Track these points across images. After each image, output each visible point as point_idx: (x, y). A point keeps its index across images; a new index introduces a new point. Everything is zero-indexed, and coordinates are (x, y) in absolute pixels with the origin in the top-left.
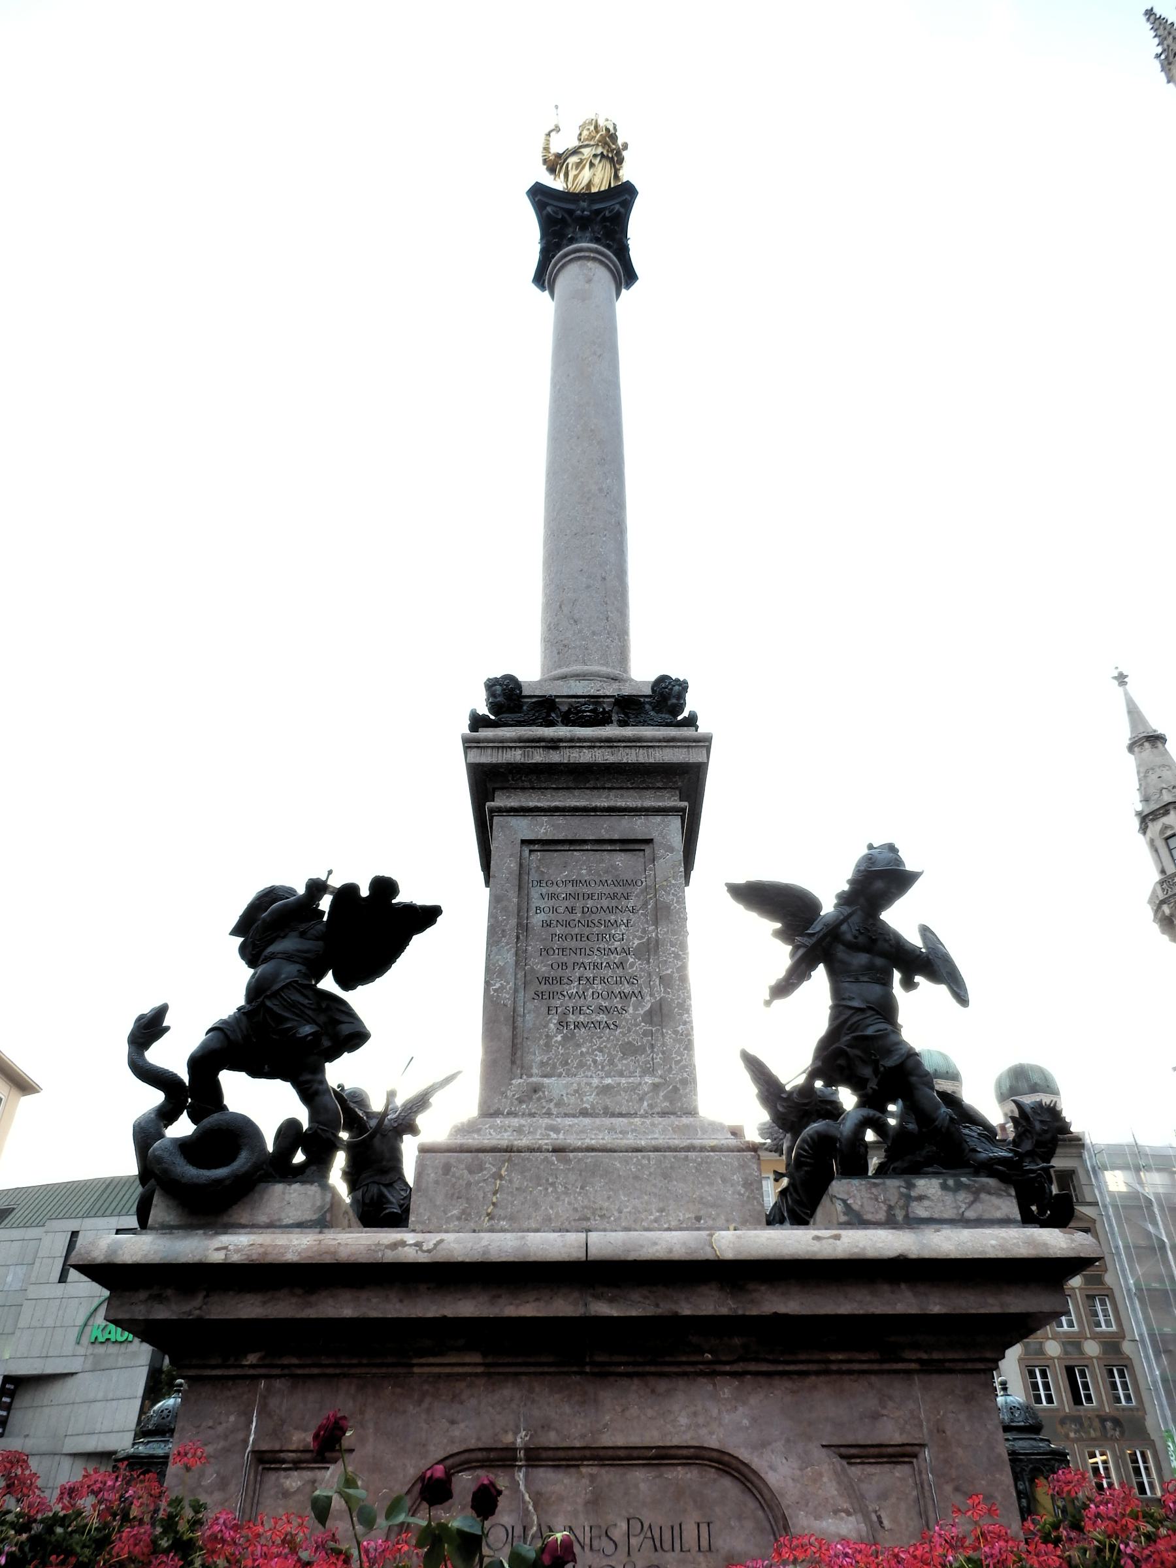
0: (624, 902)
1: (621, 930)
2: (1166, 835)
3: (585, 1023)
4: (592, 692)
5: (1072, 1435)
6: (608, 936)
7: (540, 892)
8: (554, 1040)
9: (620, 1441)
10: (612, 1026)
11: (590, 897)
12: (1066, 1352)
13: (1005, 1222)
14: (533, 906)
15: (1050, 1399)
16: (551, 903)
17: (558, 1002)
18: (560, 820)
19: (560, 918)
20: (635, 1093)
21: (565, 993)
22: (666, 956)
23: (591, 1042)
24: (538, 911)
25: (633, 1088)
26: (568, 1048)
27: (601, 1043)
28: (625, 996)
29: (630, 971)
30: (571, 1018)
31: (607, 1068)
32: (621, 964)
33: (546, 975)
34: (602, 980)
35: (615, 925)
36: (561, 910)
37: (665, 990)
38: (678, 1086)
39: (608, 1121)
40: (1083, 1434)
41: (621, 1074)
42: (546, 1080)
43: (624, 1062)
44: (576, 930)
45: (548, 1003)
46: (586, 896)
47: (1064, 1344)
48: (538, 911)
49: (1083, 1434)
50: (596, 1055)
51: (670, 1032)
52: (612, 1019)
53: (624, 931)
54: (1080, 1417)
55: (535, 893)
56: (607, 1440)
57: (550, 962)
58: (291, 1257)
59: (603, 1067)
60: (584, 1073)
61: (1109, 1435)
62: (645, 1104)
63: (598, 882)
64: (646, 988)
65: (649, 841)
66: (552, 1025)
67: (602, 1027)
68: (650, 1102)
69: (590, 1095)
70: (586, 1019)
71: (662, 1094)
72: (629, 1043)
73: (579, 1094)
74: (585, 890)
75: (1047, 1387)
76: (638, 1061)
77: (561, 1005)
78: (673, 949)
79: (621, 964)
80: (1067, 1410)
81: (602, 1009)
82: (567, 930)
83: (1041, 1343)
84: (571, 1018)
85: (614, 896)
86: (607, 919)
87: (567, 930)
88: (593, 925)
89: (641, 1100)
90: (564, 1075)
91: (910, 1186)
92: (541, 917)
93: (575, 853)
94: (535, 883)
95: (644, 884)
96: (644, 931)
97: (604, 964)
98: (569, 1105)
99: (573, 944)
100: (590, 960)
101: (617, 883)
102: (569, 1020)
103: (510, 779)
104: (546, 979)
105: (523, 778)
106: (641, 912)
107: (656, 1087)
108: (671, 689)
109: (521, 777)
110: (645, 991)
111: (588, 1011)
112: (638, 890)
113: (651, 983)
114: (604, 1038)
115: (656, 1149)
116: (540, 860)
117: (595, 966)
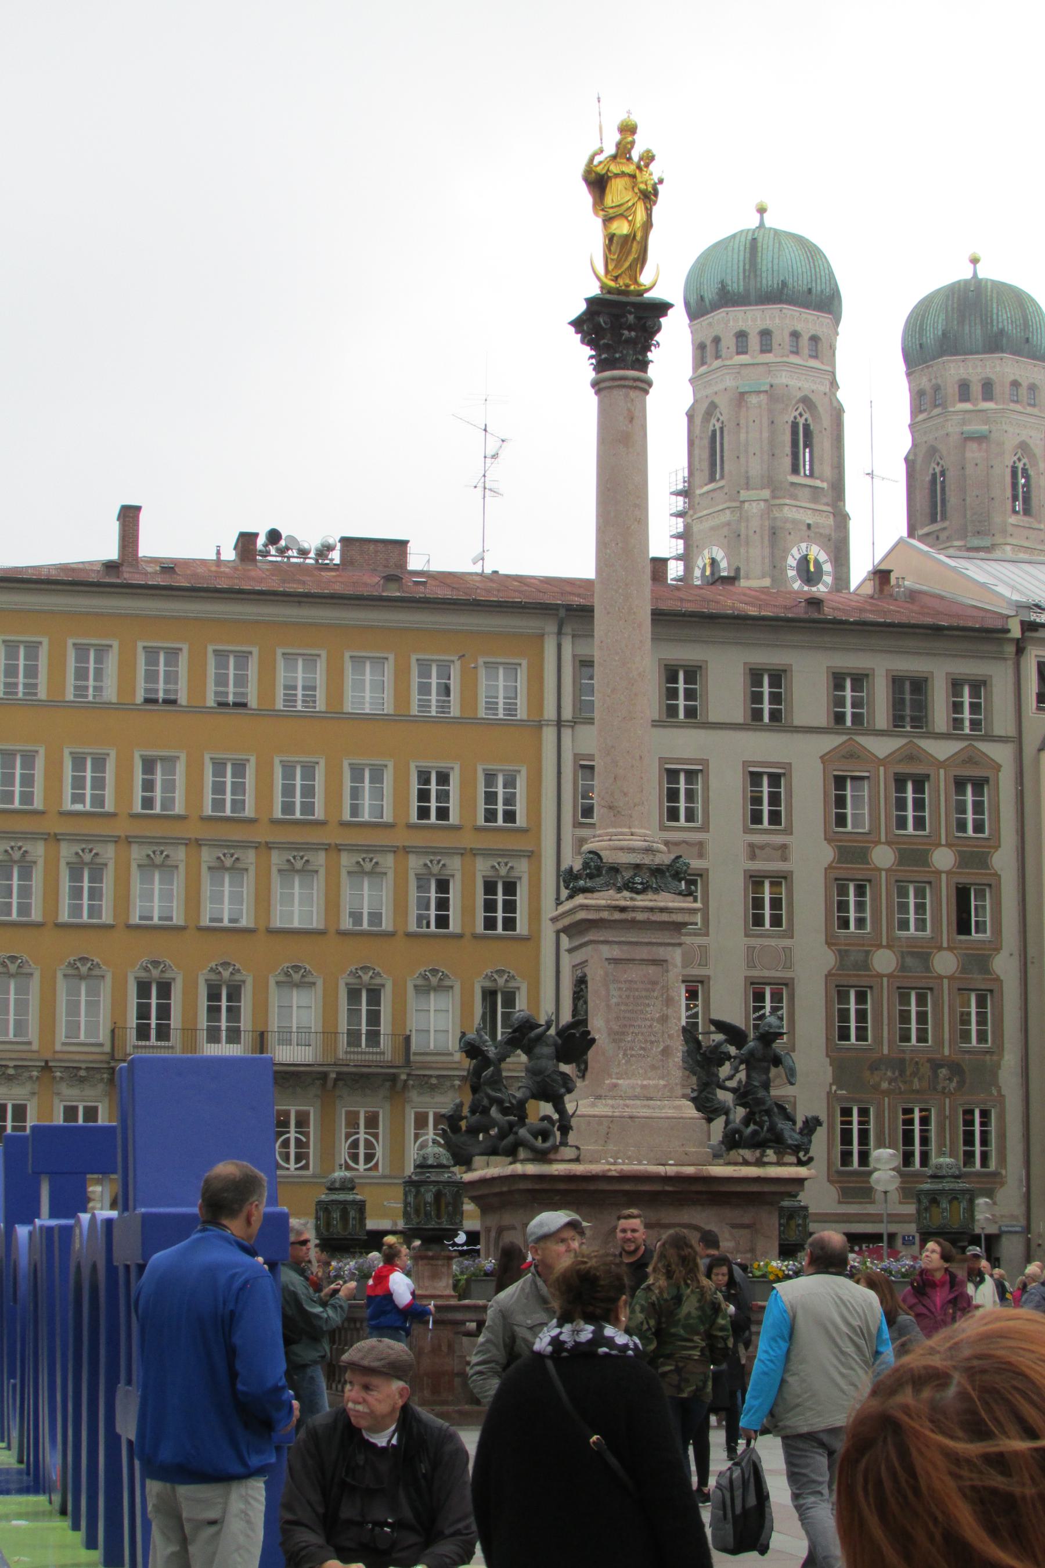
4: (638, 862)
9: (667, 1222)
11: (637, 990)
12: (903, 967)
13: (791, 1164)
15: (861, 1035)
18: (625, 948)
25: (656, 1086)
28: (652, 1042)
30: (629, 1052)
32: (651, 1026)
34: (642, 1034)
39: (646, 1102)
40: (901, 1085)
41: (649, 1079)
42: (620, 1082)
47: (902, 952)
49: (901, 1085)
54: (902, 1061)
55: (612, 987)
56: (663, 1221)
58: (578, 1173)
61: (939, 1087)
65: (666, 961)
74: (635, 986)
75: (861, 1016)
79: (651, 1026)
80: (886, 1051)
81: (642, 1048)
83: (867, 953)
91: (764, 1151)
92: (614, 1000)
99: (627, 1015)
107: (665, 1086)
112: (659, 987)
115: (668, 1118)
117: (640, 1027)
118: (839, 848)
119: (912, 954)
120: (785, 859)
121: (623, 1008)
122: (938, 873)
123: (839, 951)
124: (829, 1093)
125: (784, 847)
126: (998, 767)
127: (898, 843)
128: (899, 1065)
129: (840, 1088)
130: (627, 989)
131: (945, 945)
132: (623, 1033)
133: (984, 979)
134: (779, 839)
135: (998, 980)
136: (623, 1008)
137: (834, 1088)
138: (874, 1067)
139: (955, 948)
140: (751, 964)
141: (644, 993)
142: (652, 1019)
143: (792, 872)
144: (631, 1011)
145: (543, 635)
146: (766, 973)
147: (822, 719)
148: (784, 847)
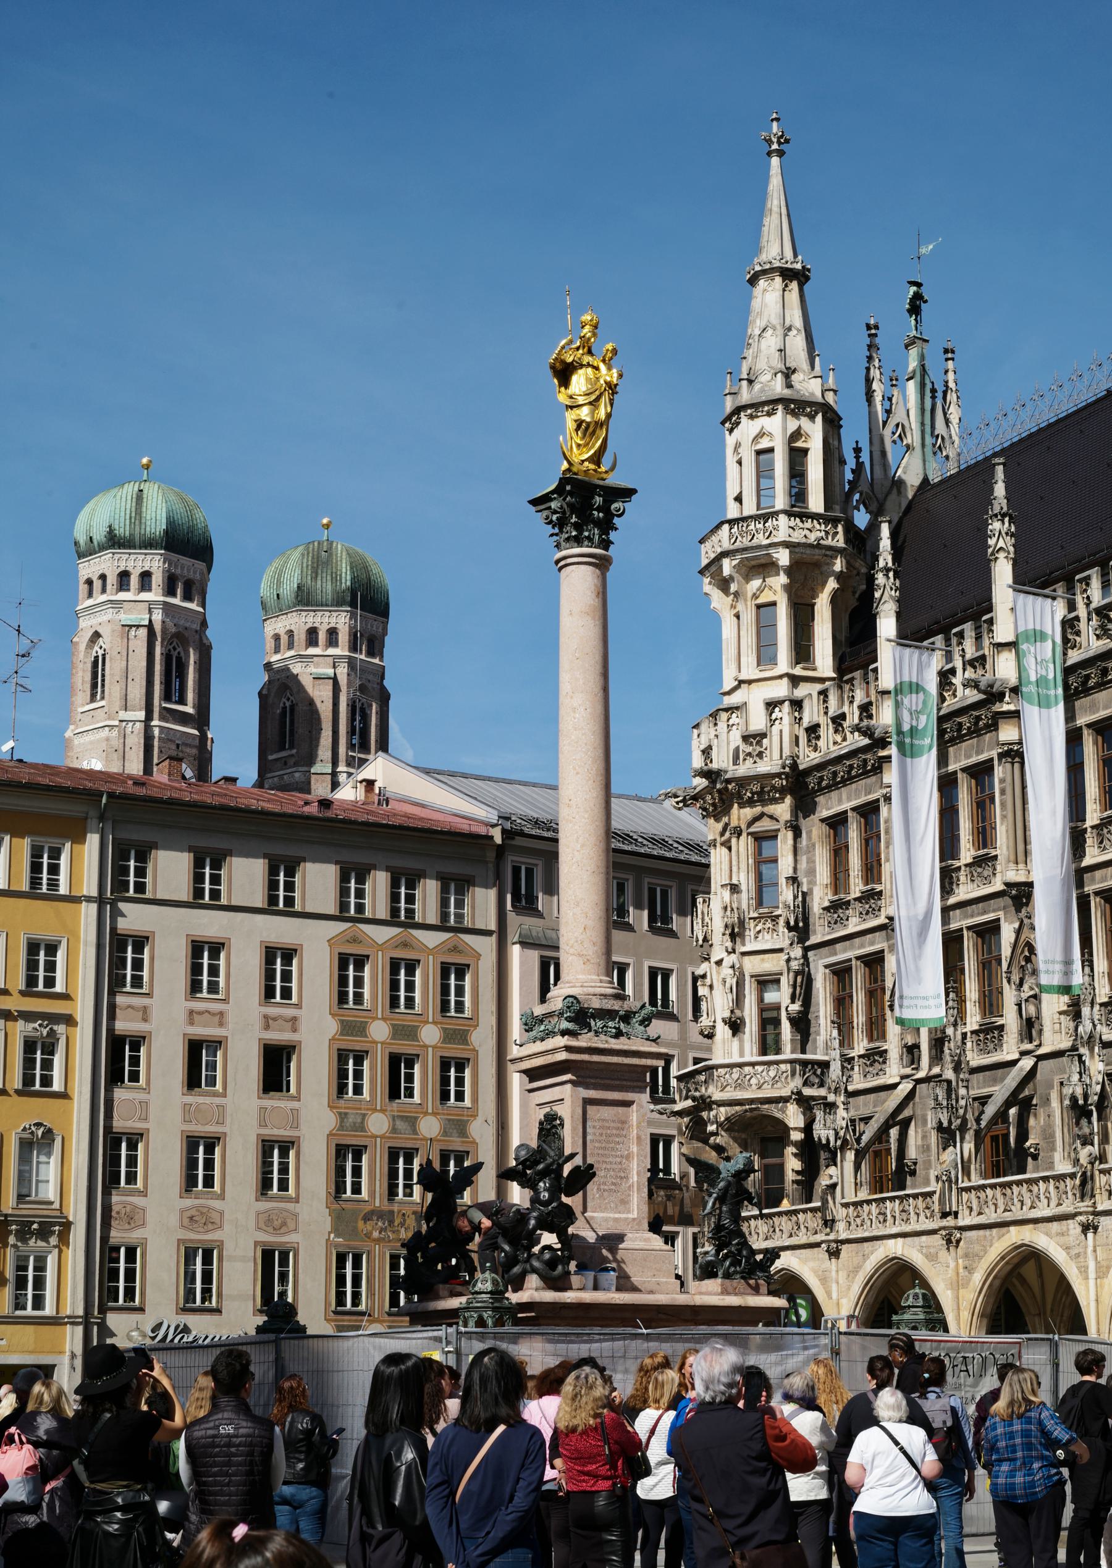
2: (760, 447)
5: (376, 1234)
11: (609, 1128)
12: (394, 1130)
28: (621, 1178)
47: (394, 1117)
81: (613, 1184)
83: (364, 1115)
85: (618, 1129)
117: (611, 1163)
118: (342, 1021)
119: (402, 1118)
120: (295, 1030)
121: (597, 1145)
122: (426, 1047)
123: (340, 1114)
124: (328, 1240)
125: (294, 1019)
126: (478, 956)
127: (392, 1019)
128: (387, 1217)
129: (336, 1236)
130: (601, 1127)
131: (430, 1111)
133: (463, 1142)
134: (290, 1012)
135: (474, 1142)
136: (597, 1145)
137: (332, 1236)
138: (367, 1218)
139: (438, 1114)
140: (263, 1124)
141: (614, 1132)
143: (300, 1042)
144: (605, 1148)
145: (86, 818)
146: (276, 1132)
147: (332, 909)
148: (294, 1019)
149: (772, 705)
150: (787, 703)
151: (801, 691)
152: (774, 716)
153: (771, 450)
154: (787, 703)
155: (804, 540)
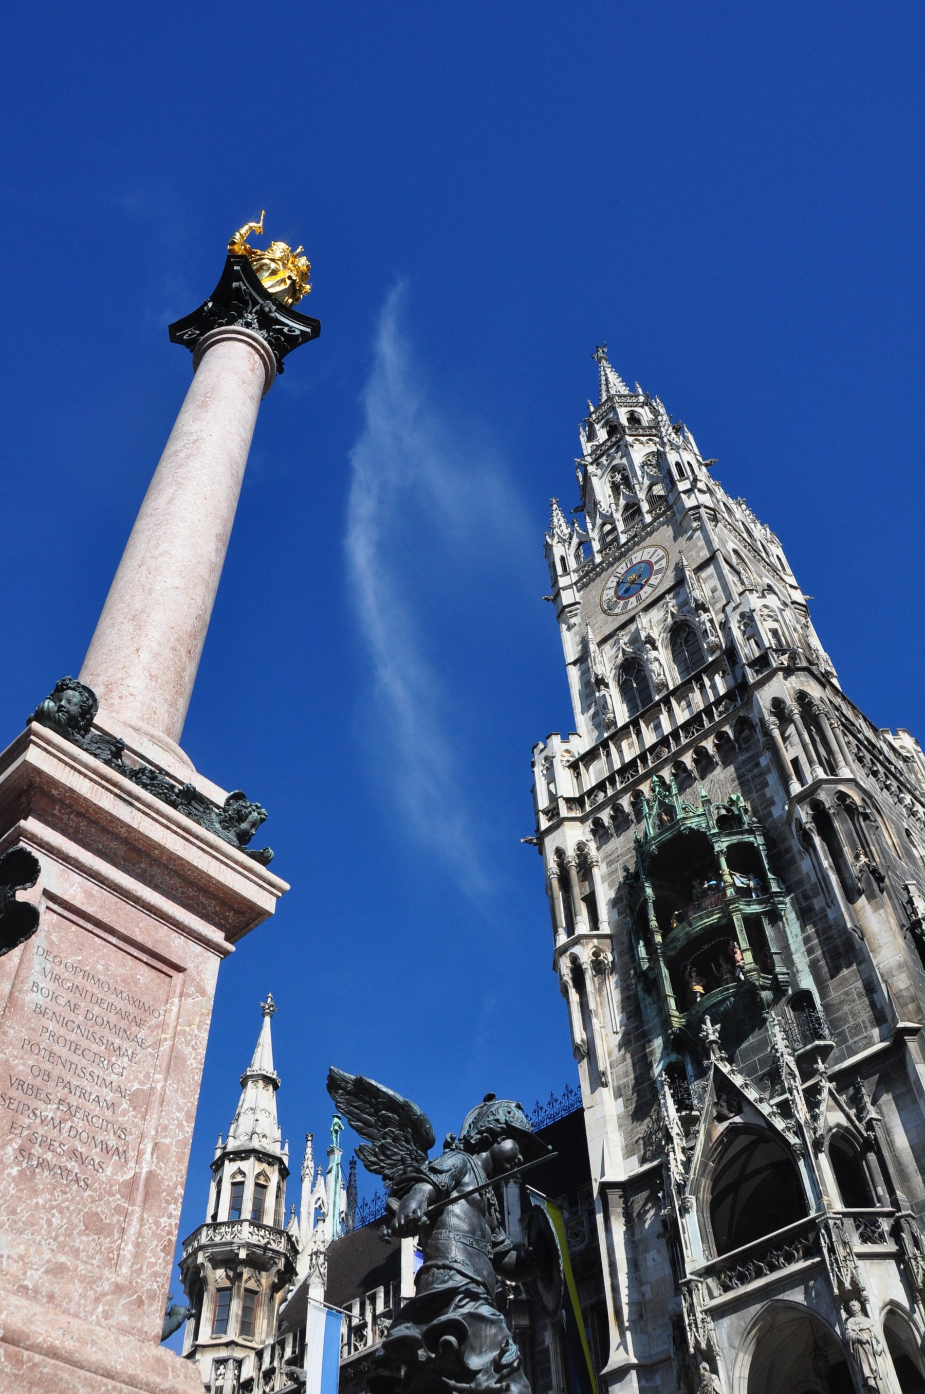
0: (134, 1029)
1: (122, 1062)
2: (235, 1180)
3: (52, 1166)
6: (106, 1062)
7: (43, 965)
8: (6, 1172)
10: (82, 1183)
11: (99, 1002)
14: (32, 979)
16: (52, 986)
17: (27, 1121)
19: (58, 1009)
20: (91, 1288)
21: (38, 1113)
22: (168, 1120)
23: (52, 1194)
24: (35, 989)
26: (22, 1191)
27: (64, 1201)
29: (120, 1119)
30: (37, 1150)
31: (61, 1239)
33: (23, 1079)
35: (117, 1052)
36: (62, 1001)
37: (158, 1162)
38: (144, 1298)
41: (76, 1253)
43: (84, 1238)
44: (73, 1037)
45: (13, 1116)
46: (94, 999)
48: (35, 989)
50: (53, 1215)
51: (151, 1221)
52: (84, 1174)
53: (126, 1065)
57: (31, 1063)
59: (57, 1236)
60: (32, 1234)
62: (100, 1309)
63: (112, 987)
64: (133, 1150)
66: (10, 1150)
67: (70, 1178)
68: (107, 1308)
69: (37, 1270)
70: (54, 1159)
71: (123, 1302)
72: (97, 1214)
73: (24, 1263)
76: (101, 1244)
77: (29, 1127)
78: (178, 1114)
79: (112, 1106)
81: (74, 1154)
82: (62, 1031)
84: (37, 1150)
86: (111, 1040)
87: (62, 1031)
88: (92, 1039)
89: (97, 1300)
90: (7, 1226)
93: (96, 939)
94: (41, 950)
95: (162, 1017)
96: (147, 1076)
97: (93, 1097)
98: (6, 1274)
100: (78, 1083)
101: (134, 1002)
102: (33, 1151)
103: (57, 808)
104: (21, 1083)
105: (72, 816)
106: (150, 1050)
107: (118, 1289)
108: (250, 813)
109: (72, 813)
110: (132, 1153)
111: (59, 1150)
113: (141, 1146)
114: (68, 1195)
116: (54, 925)
132: (36, 1092)
141: (113, 1019)
142: (119, 1090)
149: (220, 1362)
150: (231, 1361)
151: (238, 1354)
152: (219, 1372)
153: (242, 1183)
154: (231, 1361)
155: (258, 1243)
